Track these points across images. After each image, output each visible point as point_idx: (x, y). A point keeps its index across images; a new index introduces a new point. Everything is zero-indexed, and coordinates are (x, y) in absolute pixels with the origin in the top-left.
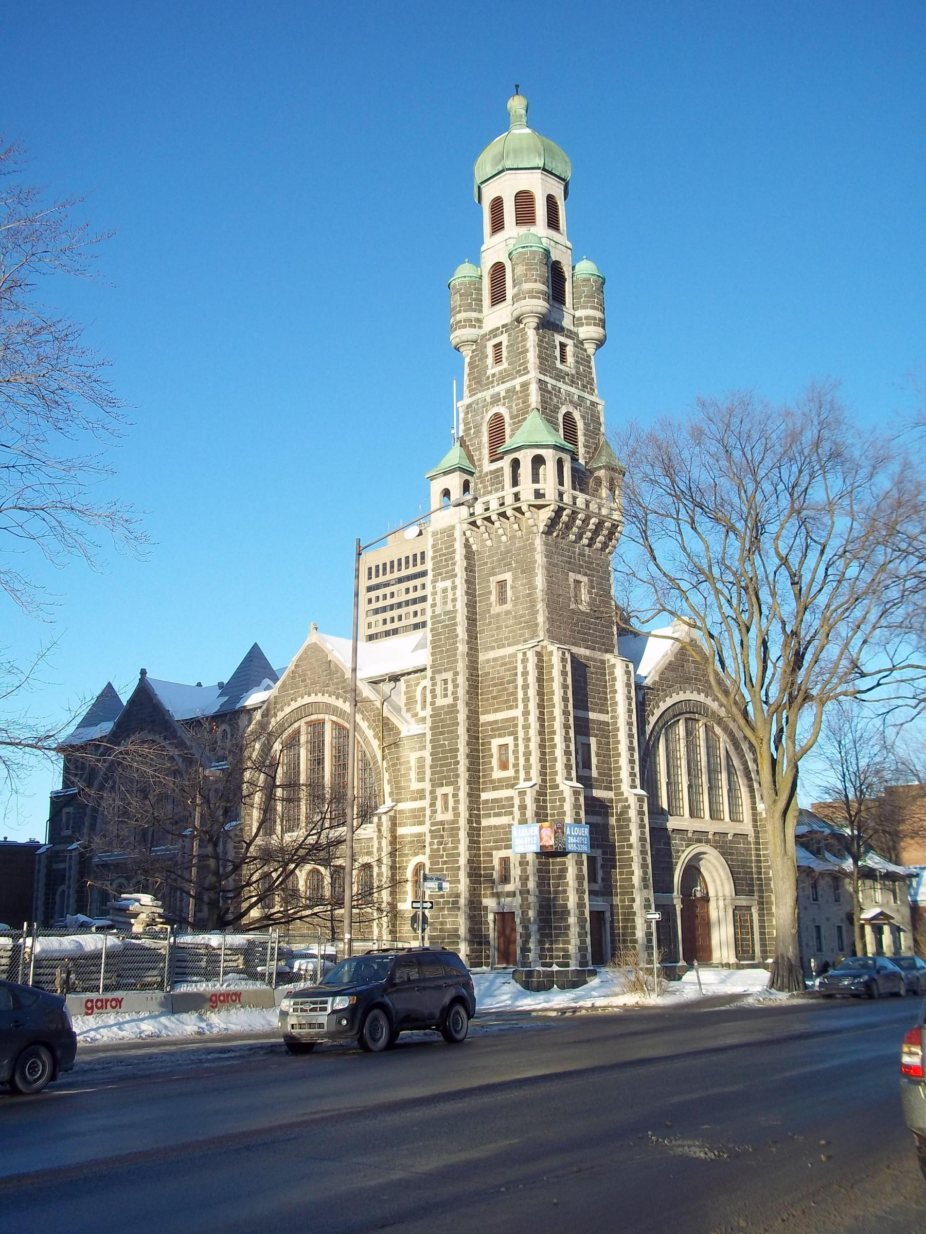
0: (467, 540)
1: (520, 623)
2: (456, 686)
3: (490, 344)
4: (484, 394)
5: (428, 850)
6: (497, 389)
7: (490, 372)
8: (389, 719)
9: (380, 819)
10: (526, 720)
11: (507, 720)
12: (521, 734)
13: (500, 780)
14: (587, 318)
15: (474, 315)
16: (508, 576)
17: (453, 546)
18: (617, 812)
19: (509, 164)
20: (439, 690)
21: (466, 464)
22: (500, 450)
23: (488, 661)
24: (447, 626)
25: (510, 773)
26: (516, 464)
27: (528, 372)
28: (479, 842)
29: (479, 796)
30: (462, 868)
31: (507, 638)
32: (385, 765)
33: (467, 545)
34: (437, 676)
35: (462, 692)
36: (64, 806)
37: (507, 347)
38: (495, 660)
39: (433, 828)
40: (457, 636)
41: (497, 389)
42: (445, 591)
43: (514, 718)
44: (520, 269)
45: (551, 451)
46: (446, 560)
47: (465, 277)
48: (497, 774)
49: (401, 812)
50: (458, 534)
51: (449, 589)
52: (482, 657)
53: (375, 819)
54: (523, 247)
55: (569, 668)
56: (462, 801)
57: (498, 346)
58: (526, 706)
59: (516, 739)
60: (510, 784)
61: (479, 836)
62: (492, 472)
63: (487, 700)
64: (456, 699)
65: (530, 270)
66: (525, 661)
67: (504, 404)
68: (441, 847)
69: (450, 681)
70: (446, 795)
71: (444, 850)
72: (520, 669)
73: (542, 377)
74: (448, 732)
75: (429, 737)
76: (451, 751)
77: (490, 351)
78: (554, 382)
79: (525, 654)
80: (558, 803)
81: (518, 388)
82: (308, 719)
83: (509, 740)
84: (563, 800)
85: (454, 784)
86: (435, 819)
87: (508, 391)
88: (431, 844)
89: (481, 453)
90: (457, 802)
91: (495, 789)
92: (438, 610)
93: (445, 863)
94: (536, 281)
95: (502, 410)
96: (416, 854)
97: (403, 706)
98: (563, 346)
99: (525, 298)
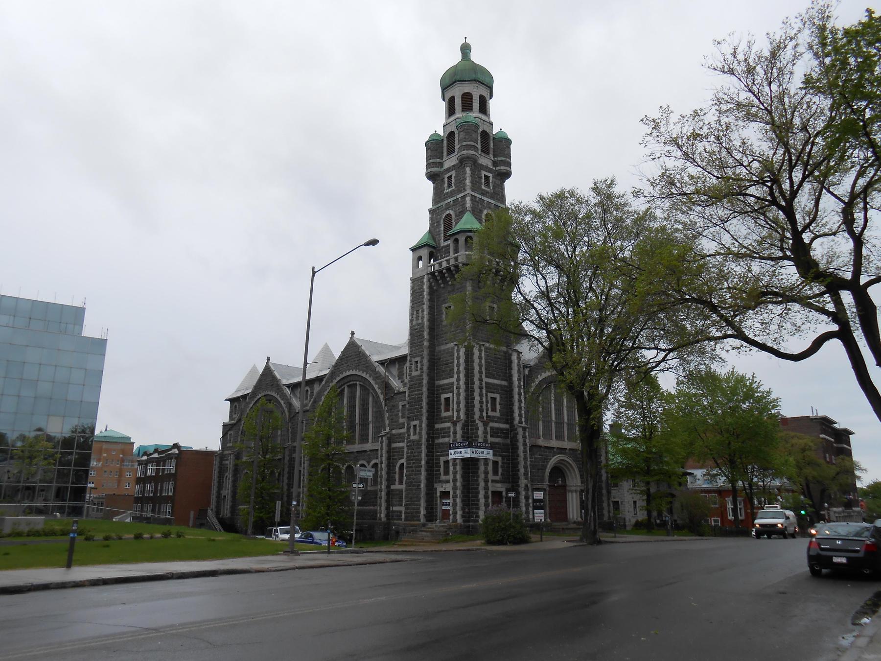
0: (431, 284)
2: (422, 365)
3: (446, 176)
4: (442, 204)
5: (405, 456)
6: (449, 201)
7: (445, 192)
9: (382, 439)
10: (458, 384)
11: (449, 384)
12: (455, 391)
13: (445, 418)
15: (438, 160)
17: (423, 288)
19: (458, 78)
21: (432, 242)
22: (449, 233)
26: (456, 241)
27: (466, 191)
28: (433, 452)
30: (423, 466)
33: (430, 287)
35: (425, 368)
38: (444, 350)
40: (424, 337)
41: (449, 201)
44: (462, 135)
48: (444, 414)
50: (425, 280)
52: (437, 349)
53: (380, 439)
55: (483, 355)
56: (424, 429)
57: (450, 178)
58: (458, 377)
64: (422, 372)
66: (458, 351)
72: (456, 354)
73: (473, 193)
74: (418, 390)
78: (480, 196)
82: (348, 384)
83: (450, 395)
84: (478, 429)
89: (440, 237)
90: (421, 429)
91: (442, 422)
92: (414, 323)
93: (414, 463)
95: (451, 212)
98: (487, 177)
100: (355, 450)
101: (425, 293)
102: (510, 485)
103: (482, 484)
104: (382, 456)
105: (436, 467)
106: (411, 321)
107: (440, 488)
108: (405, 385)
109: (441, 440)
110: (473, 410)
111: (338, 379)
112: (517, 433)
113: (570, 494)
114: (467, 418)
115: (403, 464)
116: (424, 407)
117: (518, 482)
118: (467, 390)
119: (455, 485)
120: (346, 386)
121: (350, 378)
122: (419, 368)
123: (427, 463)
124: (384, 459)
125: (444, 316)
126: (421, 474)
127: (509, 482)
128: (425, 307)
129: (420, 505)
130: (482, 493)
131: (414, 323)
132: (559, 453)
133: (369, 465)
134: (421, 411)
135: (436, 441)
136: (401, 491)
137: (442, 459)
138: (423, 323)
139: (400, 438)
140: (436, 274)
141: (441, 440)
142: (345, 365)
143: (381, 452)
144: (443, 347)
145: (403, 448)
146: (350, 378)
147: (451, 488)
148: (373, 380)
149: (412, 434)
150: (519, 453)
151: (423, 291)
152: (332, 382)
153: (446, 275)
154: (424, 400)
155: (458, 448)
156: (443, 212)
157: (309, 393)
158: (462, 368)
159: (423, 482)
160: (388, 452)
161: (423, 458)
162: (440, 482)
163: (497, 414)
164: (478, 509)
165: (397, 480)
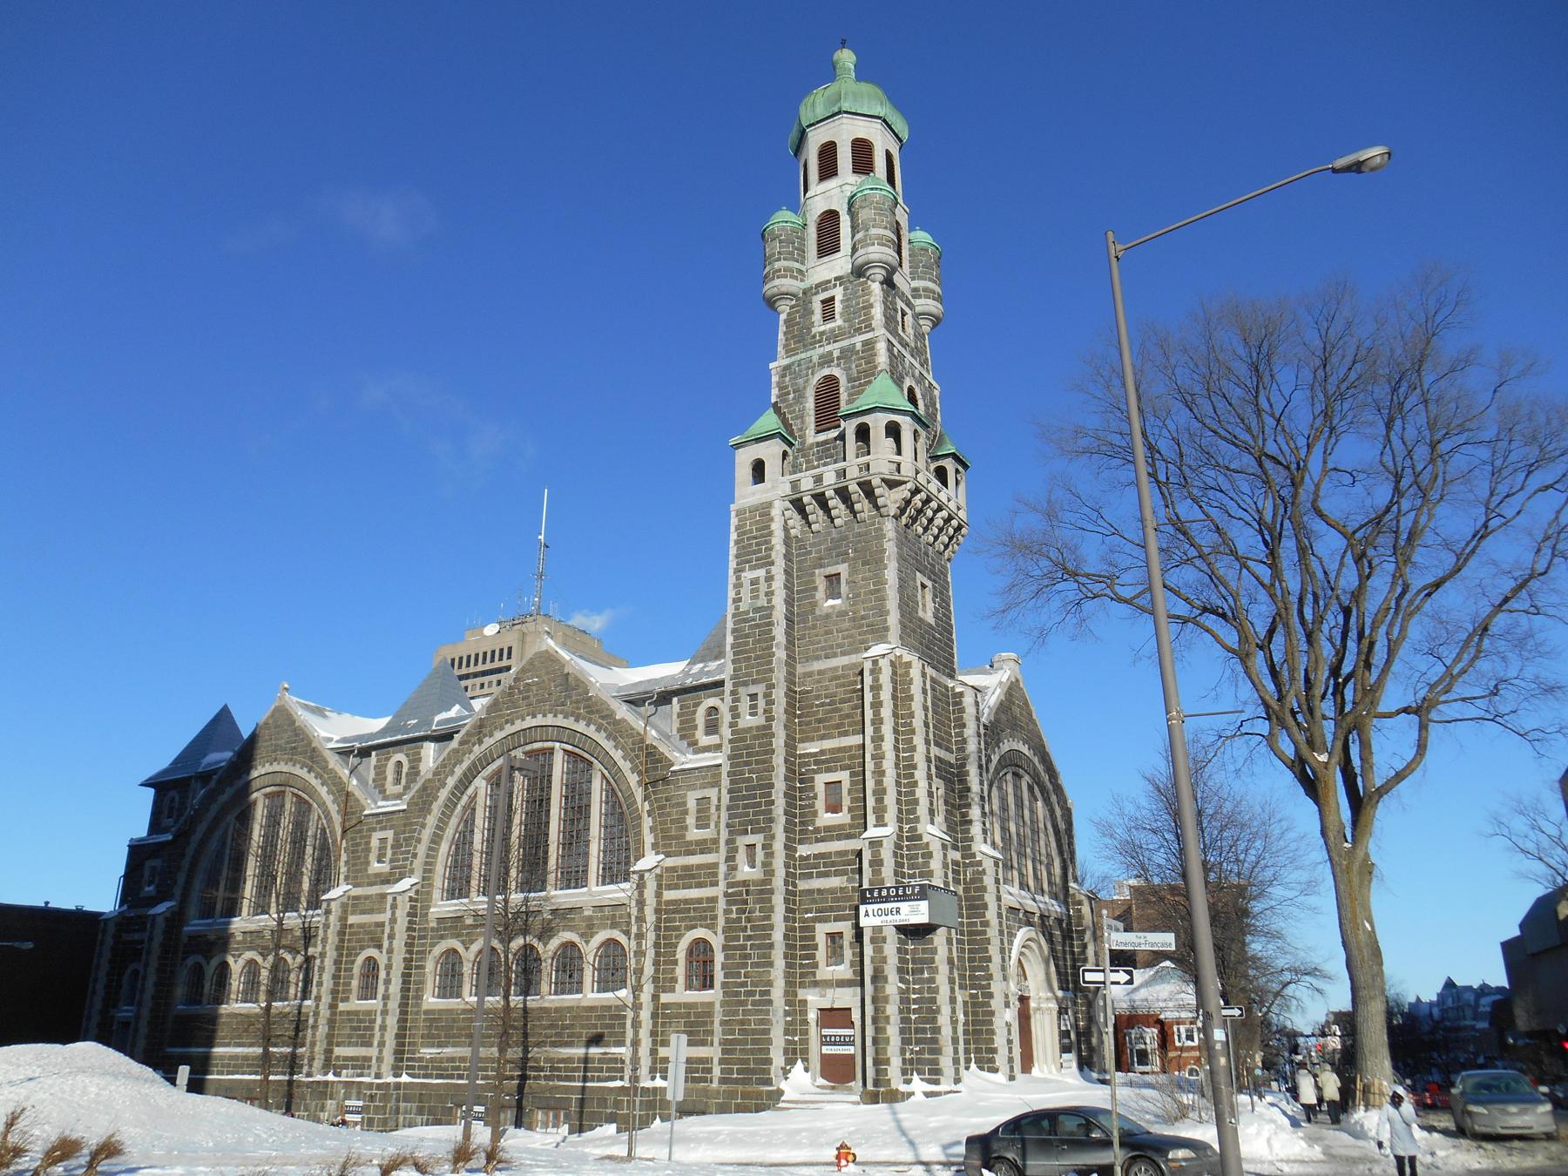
2: (770, 702)
5: (721, 922)
6: (828, 348)
8: (655, 748)
13: (828, 829)
14: (925, 290)
15: (797, 265)
16: (843, 569)
24: (758, 626)
31: (839, 646)
32: (647, 806)
34: (741, 690)
35: (779, 709)
36: (148, 858)
37: (842, 301)
38: (820, 672)
39: (730, 891)
41: (828, 348)
42: (754, 582)
45: (908, 419)
46: (757, 544)
47: (786, 222)
48: (825, 819)
50: (776, 512)
51: (762, 580)
52: (800, 669)
54: (872, 189)
62: (818, 444)
63: (809, 723)
64: (770, 719)
65: (880, 214)
66: (876, 671)
67: (838, 365)
68: (743, 916)
69: (760, 697)
71: (748, 920)
75: (725, 769)
76: (761, 787)
77: (817, 307)
79: (875, 662)
81: (859, 347)
82: (528, 748)
84: (930, 855)
85: (766, 829)
86: (734, 877)
87: (843, 350)
88: (727, 912)
90: (770, 856)
92: (743, 607)
93: (749, 938)
94: (886, 228)
99: (873, 244)
111: (499, 735)
122: (760, 710)
126: (771, 964)
136: (706, 1011)
139: (706, 876)
145: (713, 900)
148: (608, 738)
152: (480, 742)
155: (887, 900)
156: (812, 368)
157: (405, 770)
158: (886, 712)
162: (816, 984)
164: (938, 1051)
165: (681, 980)
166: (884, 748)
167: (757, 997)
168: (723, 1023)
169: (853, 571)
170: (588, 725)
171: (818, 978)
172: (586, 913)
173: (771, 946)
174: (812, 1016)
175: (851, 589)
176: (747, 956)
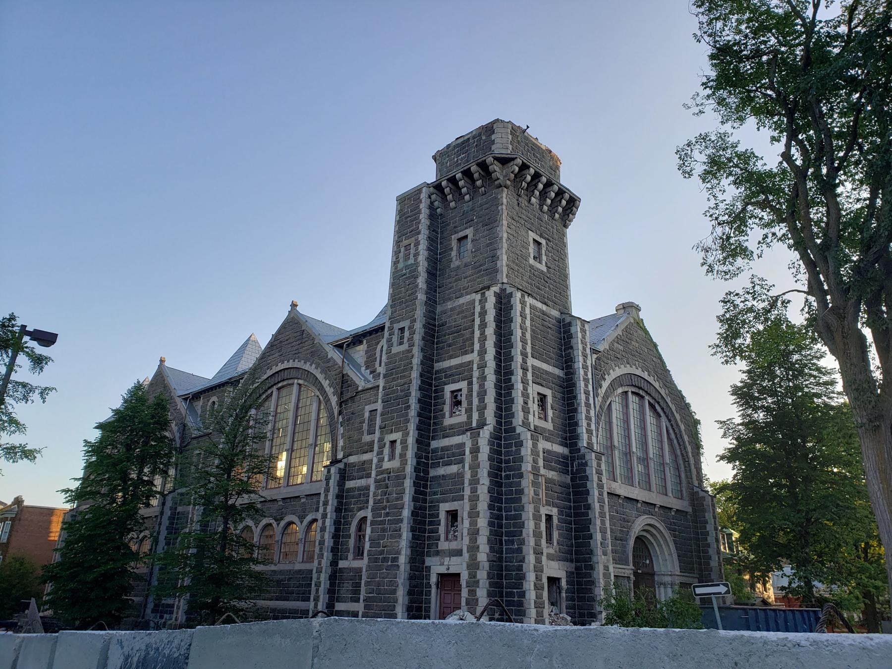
0: (432, 203)
1: (480, 271)
8: (348, 376)
11: (461, 365)
13: (452, 427)
18: (572, 470)
20: (395, 339)
23: (445, 312)
25: (460, 418)
29: (429, 445)
31: (464, 289)
32: (341, 420)
33: (431, 207)
35: (417, 338)
38: (452, 309)
39: (378, 478)
40: (417, 286)
43: (471, 363)
46: (411, 221)
49: (353, 465)
50: (424, 196)
51: (412, 245)
52: (439, 309)
59: (470, 384)
60: (465, 428)
61: (425, 486)
64: (412, 345)
68: (385, 497)
69: (406, 329)
70: (393, 442)
80: (514, 448)
83: (463, 385)
84: (520, 444)
88: (375, 495)
90: (405, 448)
92: (401, 265)
96: (360, 509)
97: (363, 364)
100: (279, 497)
101: (422, 216)
102: (573, 565)
103: (531, 559)
104: (326, 503)
105: (431, 523)
106: (395, 263)
107: (437, 567)
108: (377, 376)
109: (441, 471)
110: (509, 409)
112: (586, 464)
113: (662, 589)
114: (499, 423)
115: (364, 519)
116: (413, 407)
117: (590, 559)
118: (498, 372)
119: (473, 557)
120: (274, 389)
121: (286, 374)
123: (414, 514)
124: (329, 508)
125: (454, 253)
126: (400, 536)
127: (572, 561)
128: (423, 238)
129: (396, 601)
130: (531, 577)
131: (401, 265)
132: (645, 513)
133: (302, 522)
134: (407, 415)
135: (433, 473)
137: (444, 507)
138: (416, 264)
140: (444, 183)
141: (441, 471)
142: (277, 355)
143: (326, 496)
144: (449, 305)
146: (286, 374)
147: (465, 566)
149: (386, 459)
150: (590, 501)
151: (420, 212)
153: (461, 183)
154: (413, 394)
158: (490, 330)
159: (403, 552)
160: (339, 497)
161: (407, 503)
162: (437, 553)
163: (549, 426)
165: (351, 550)
166: (486, 359)
167: (390, 563)
168: (367, 583)
169: (476, 231)
170: (311, 365)
171: (439, 548)
172: (303, 500)
173: (401, 521)
174: (433, 579)
175: (474, 246)
176: (384, 530)
